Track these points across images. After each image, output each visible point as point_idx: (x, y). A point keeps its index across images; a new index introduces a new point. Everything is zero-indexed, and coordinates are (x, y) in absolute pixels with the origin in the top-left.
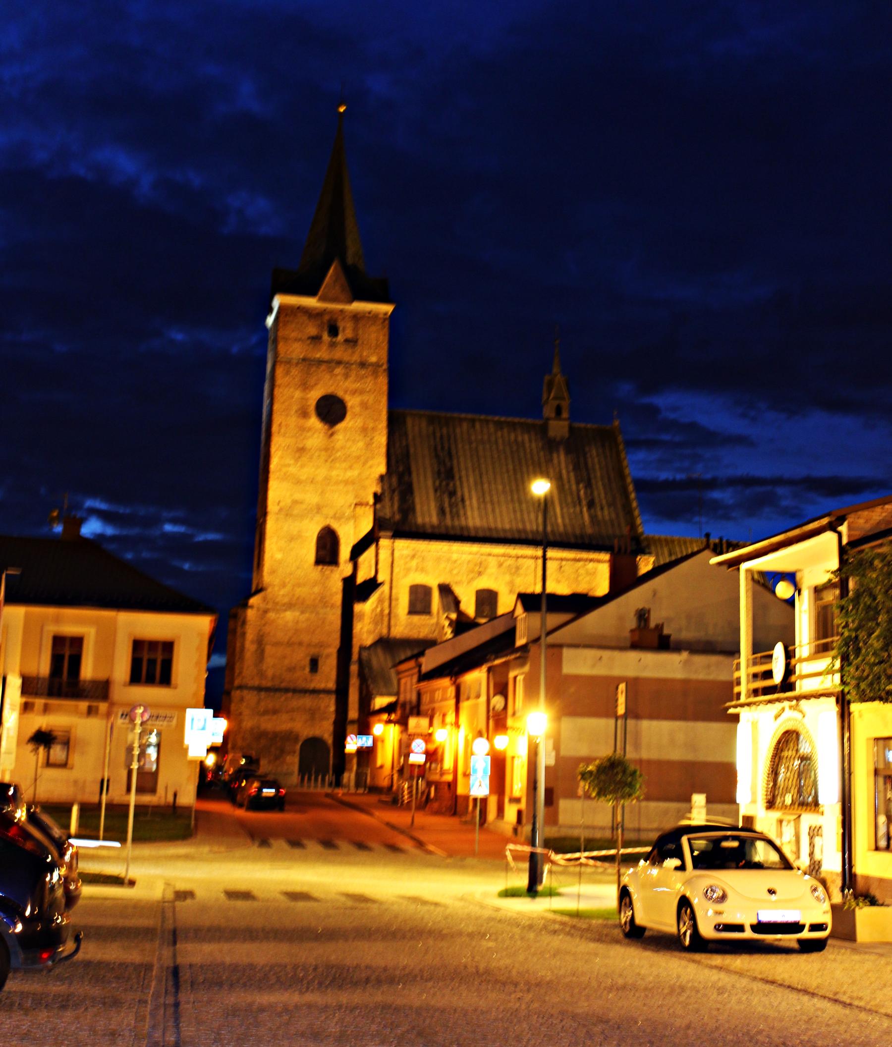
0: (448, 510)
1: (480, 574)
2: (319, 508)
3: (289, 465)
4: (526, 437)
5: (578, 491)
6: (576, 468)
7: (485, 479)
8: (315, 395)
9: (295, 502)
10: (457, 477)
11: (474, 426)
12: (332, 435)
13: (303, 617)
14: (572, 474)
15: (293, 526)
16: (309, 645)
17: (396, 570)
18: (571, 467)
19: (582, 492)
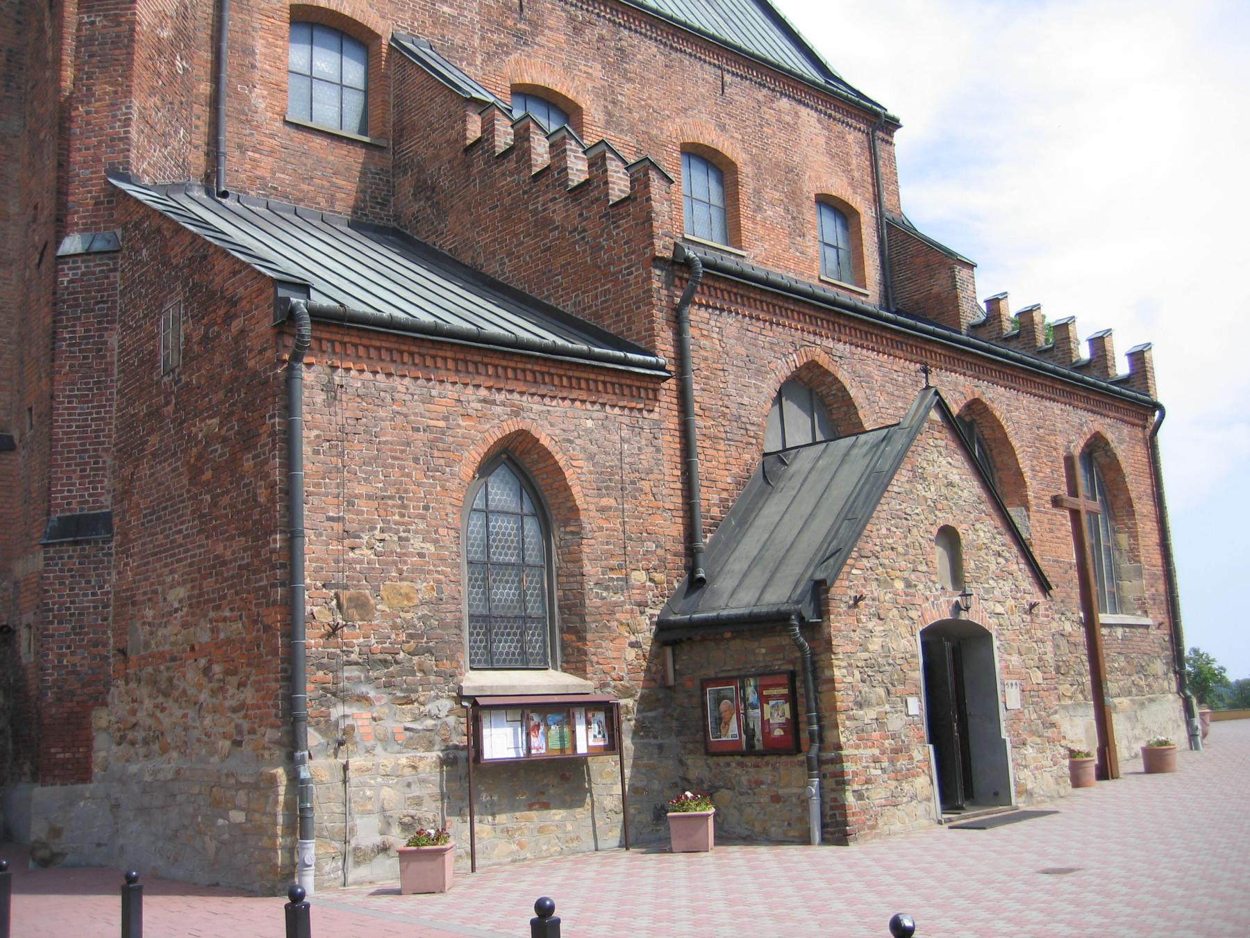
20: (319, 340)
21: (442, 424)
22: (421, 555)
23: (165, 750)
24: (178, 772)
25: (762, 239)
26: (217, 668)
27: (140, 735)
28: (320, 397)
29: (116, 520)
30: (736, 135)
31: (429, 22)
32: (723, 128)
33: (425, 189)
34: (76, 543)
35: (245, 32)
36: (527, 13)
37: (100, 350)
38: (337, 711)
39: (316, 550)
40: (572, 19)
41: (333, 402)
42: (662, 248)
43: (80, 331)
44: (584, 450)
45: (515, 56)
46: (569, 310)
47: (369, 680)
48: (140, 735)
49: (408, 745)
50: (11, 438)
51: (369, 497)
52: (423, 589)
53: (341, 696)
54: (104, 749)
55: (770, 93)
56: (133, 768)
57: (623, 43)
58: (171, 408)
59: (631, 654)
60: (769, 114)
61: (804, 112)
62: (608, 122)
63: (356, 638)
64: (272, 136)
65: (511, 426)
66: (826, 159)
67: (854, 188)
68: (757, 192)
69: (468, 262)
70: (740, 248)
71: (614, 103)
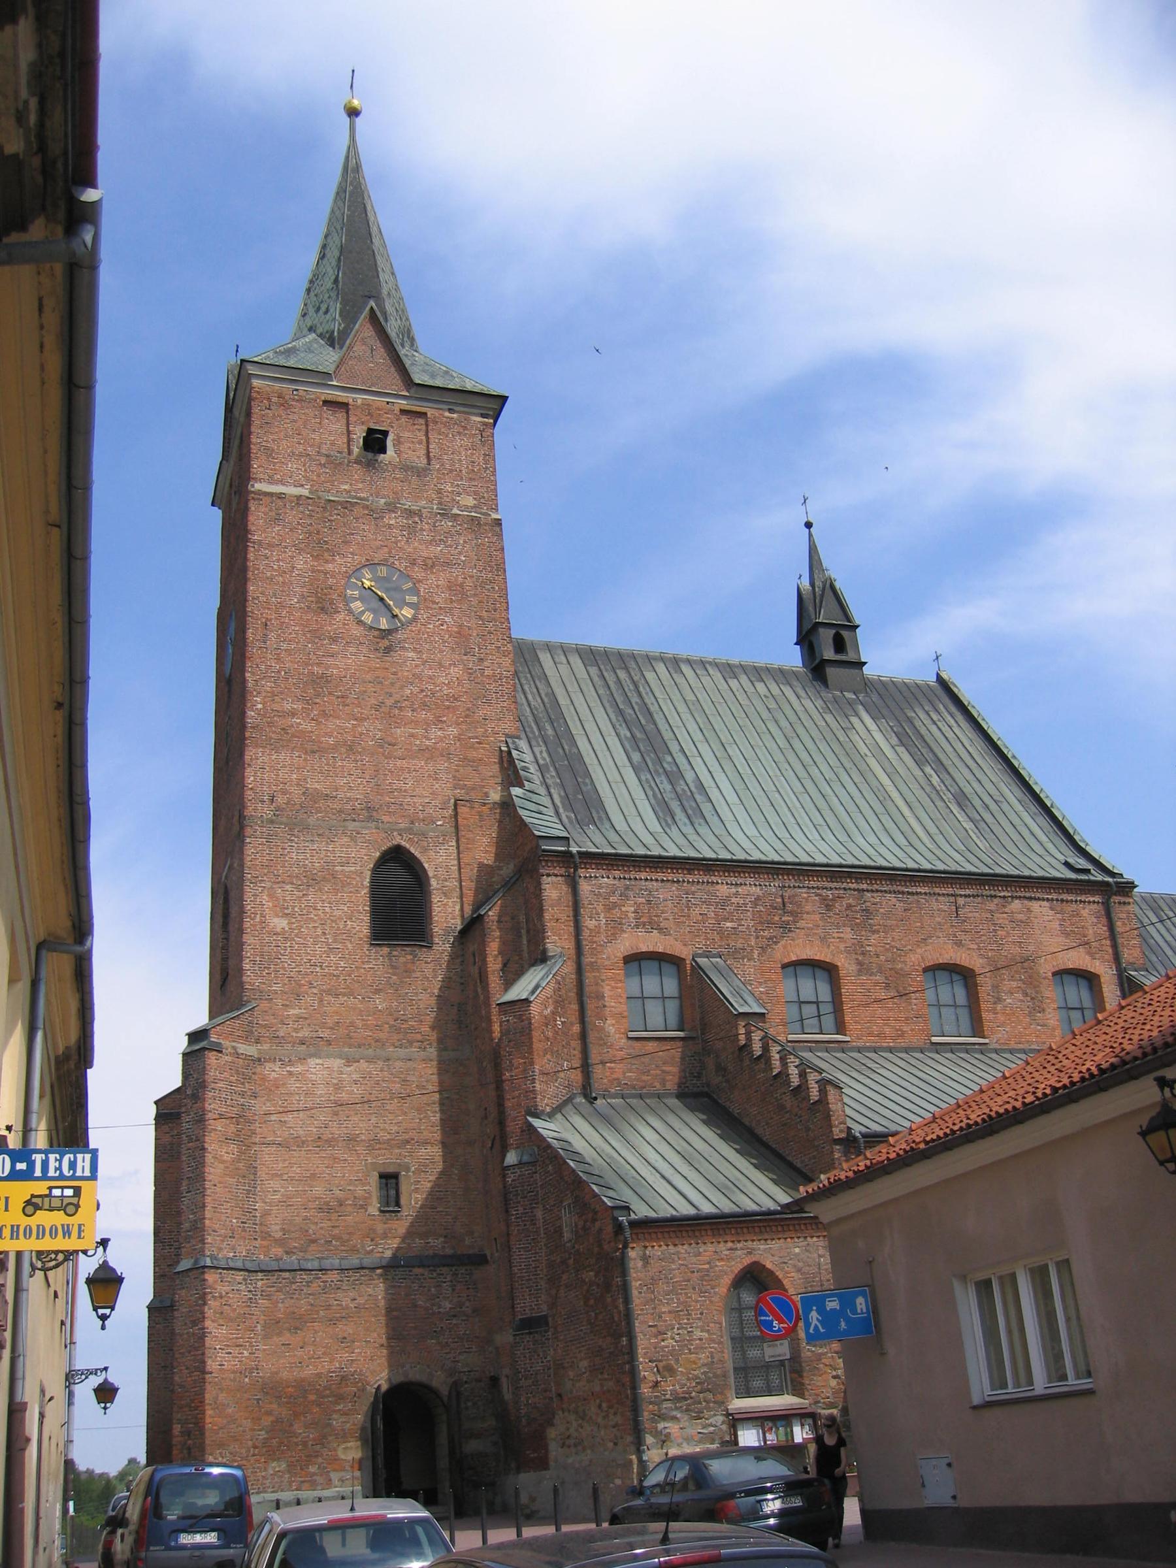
0: (675, 805)
1: (786, 928)
2: (370, 812)
3: (293, 714)
9: (313, 797)
10: (674, 747)
12: (388, 650)
13: (351, 1073)
14: (901, 749)
15: (306, 853)
16: (374, 1144)
17: (589, 923)
19: (935, 780)
20: (637, 1234)
21: (707, 1266)
22: (701, 1339)
23: (584, 1449)
24: (591, 1461)
25: (1002, 1025)
26: (604, 1405)
27: (572, 1441)
28: (640, 1264)
29: (550, 1319)
30: (972, 946)
31: (717, 938)
32: (959, 944)
33: (721, 1069)
34: (530, 1333)
35: (597, 984)
36: (789, 907)
37: (533, 1221)
38: (661, 1426)
39: (644, 1343)
40: (824, 899)
41: (645, 1263)
42: (838, 1133)
43: (521, 1210)
44: (795, 1266)
45: (783, 942)
46: (799, 1165)
47: (677, 1408)
48: (572, 1441)
49: (700, 1442)
50: (485, 1256)
51: (670, 1312)
52: (703, 1357)
53: (663, 1417)
54: (554, 1450)
55: (1001, 900)
56: (570, 1461)
57: (868, 904)
58: (571, 1261)
59: (833, 1383)
60: (1001, 919)
61: (1035, 905)
62: (860, 971)
63: (668, 1388)
64: (621, 1049)
65: (747, 1261)
66: (1062, 939)
67: (1092, 955)
68: (996, 987)
69: (747, 1123)
70: (984, 1037)
71: (863, 954)
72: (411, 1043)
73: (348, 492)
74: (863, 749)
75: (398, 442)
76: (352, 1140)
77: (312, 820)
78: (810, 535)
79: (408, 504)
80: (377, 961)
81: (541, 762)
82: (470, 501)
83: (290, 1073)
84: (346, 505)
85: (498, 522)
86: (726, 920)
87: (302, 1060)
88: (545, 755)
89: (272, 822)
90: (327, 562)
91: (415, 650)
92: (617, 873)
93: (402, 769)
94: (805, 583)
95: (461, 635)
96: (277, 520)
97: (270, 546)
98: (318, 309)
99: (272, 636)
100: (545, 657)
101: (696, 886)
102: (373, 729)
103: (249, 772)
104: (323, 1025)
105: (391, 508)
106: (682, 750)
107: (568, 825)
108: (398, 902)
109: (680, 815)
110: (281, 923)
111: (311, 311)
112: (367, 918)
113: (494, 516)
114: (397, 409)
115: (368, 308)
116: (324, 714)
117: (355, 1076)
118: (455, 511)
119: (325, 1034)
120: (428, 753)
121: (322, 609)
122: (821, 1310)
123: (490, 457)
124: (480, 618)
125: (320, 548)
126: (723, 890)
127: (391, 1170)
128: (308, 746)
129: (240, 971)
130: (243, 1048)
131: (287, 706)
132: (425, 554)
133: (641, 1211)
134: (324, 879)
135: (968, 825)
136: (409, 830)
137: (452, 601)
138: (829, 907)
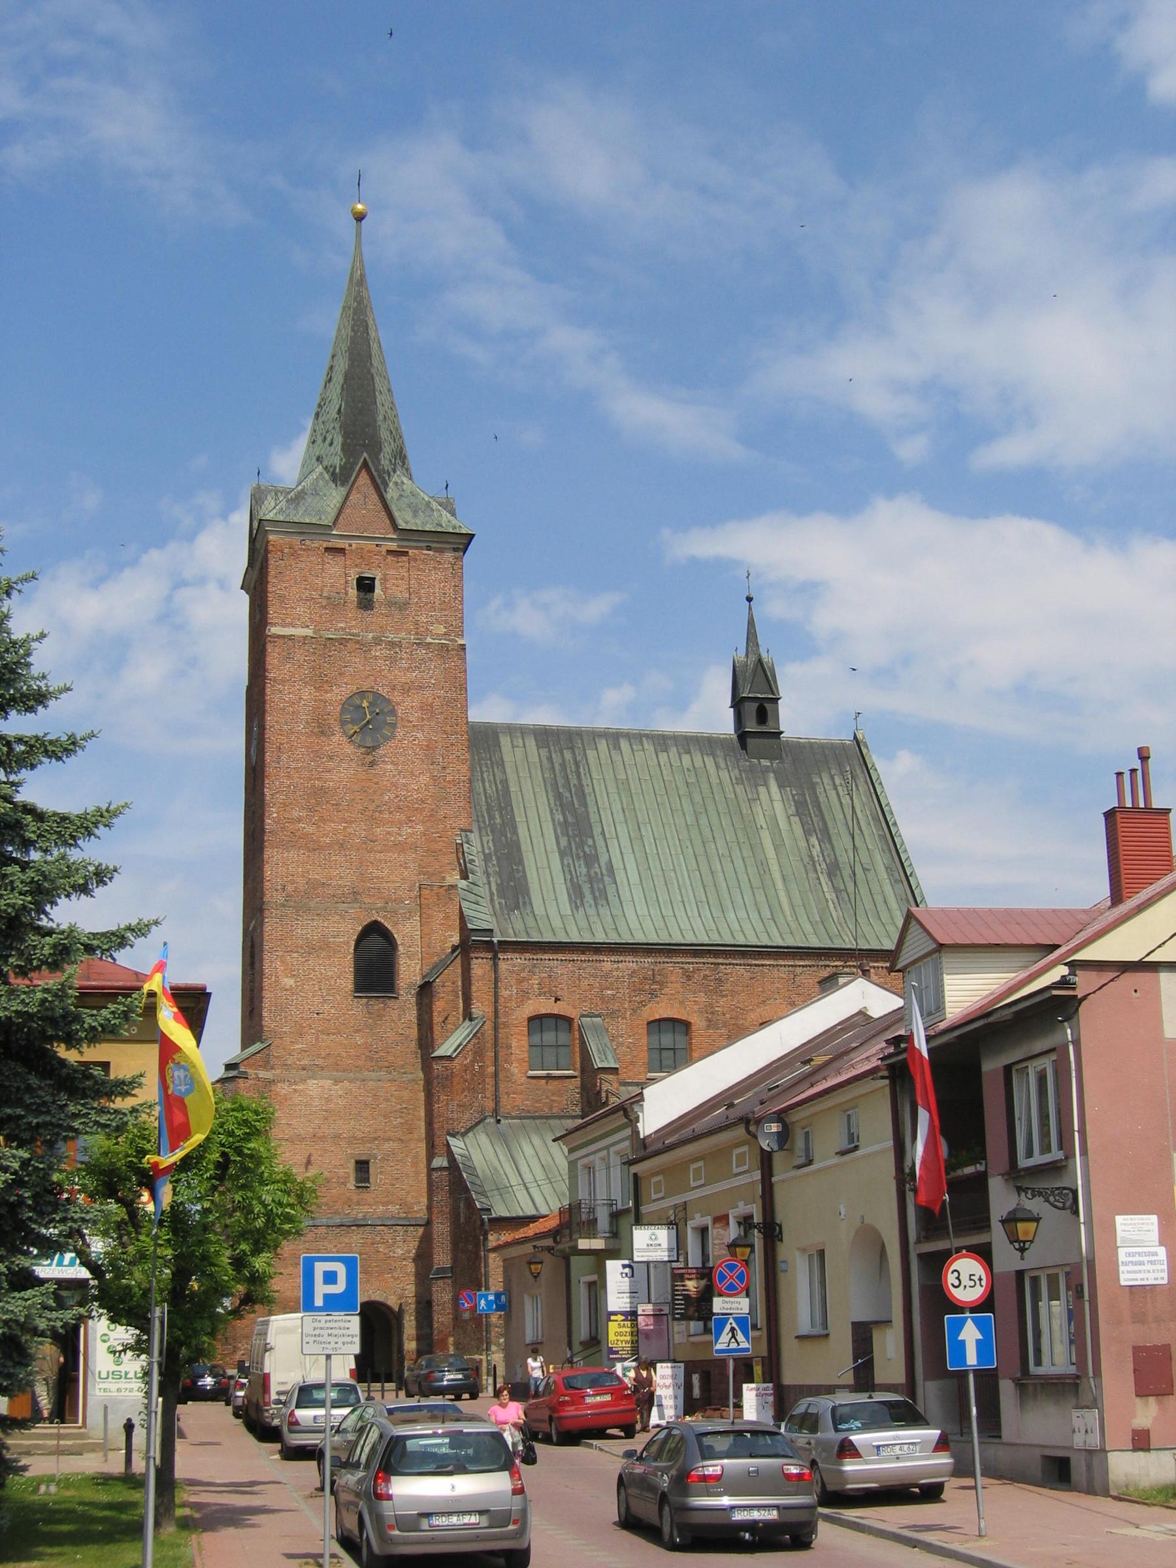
0: (586, 889)
1: (653, 994)
3: (299, 820)
4: (709, 761)
5: (809, 847)
6: (801, 809)
7: (646, 832)
8: (339, 694)
9: (314, 885)
10: (597, 830)
11: (617, 747)
12: (372, 764)
13: (338, 1089)
15: (308, 929)
16: (352, 1140)
17: (504, 993)
18: (792, 810)
19: (816, 851)
36: (658, 978)
40: (685, 971)
62: (708, 1026)
71: (712, 1013)
72: (380, 1068)
73: (343, 629)
74: (761, 821)
75: (385, 580)
76: (337, 1136)
77: (312, 904)
78: (750, 608)
79: (391, 637)
80: (357, 1009)
81: (487, 851)
82: (442, 629)
83: (295, 1090)
84: (343, 642)
85: (463, 647)
86: (608, 989)
87: (303, 1081)
88: (491, 844)
89: (284, 906)
90: (326, 692)
91: (393, 763)
92: (528, 956)
93: (380, 861)
94: (741, 655)
95: (429, 747)
96: (288, 658)
97: (283, 681)
98: (325, 439)
99: (284, 757)
100: (505, 741)
101: (586, 964)
102: (358, 830)
103: (267, 867)
104: (319, 1056)
105: (377, 641)
106: (603, 833)
107: (499, 912)
108: (375, 964)
109: (588, 898)
110: (289, 982)
111: (319, 439)
112: (351, 977)
113: (461, 642)
114: (383, 550)
115: (362, 460)
116: (322, 819)
117: (340, 1093)
118: (429, 640)
119: (319, 1062)
120: (401, 847)
121: (322, 732)
122: (486, 1300)
123: (458, 588)
124: (445, 732)
125: (321, 682)
126: (607, 966)
127: (363, 1158)
128: (311, 845)
129: (261, 1009)
130: (262, 1074)
131: (295, 814)
132: (403, 680)
133: (500, 1211)
134: (321, 948)
135: (830, 895)
136: (384, 909)
137: (423, 719)
138: (689, 978)
